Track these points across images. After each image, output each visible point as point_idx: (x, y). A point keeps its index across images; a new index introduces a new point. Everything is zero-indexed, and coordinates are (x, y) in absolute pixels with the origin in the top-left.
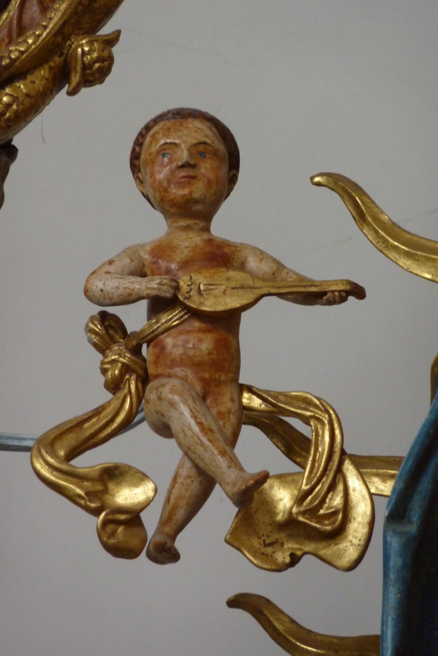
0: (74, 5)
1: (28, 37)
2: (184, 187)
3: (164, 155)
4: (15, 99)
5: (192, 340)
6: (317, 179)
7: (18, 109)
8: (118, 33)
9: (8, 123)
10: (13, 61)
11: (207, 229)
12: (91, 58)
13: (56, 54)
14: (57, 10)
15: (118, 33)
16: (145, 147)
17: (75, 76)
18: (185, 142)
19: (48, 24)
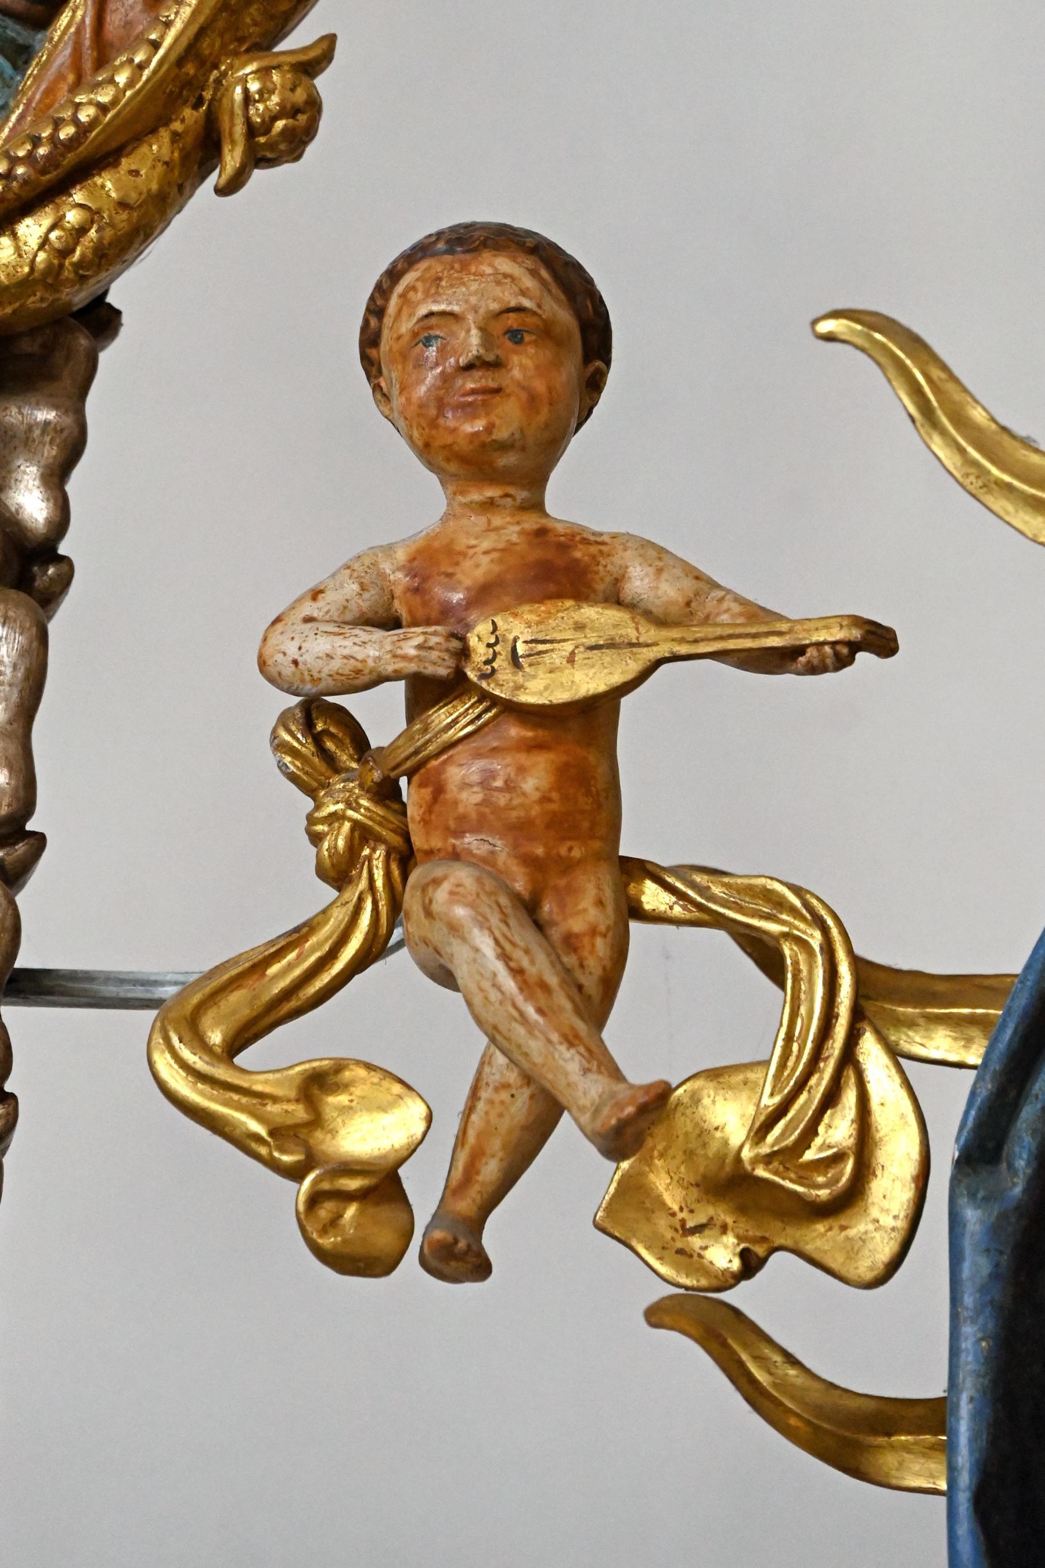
1: (117, 70)
2: (474, 417)
3: (427, 342)
4: (93, 214)
5: (502, 767)
6: (826, 326)
7: (100, 239)
8: (330, 40)
9: (81, 272)
10: (83, 130)
11: (538, 506)
12: (266, 108)
13: (185, 102)
15: (330, 40)
16: (387, 321)
17: (231, 151)
18: (475, 310)
19: (162, 37)
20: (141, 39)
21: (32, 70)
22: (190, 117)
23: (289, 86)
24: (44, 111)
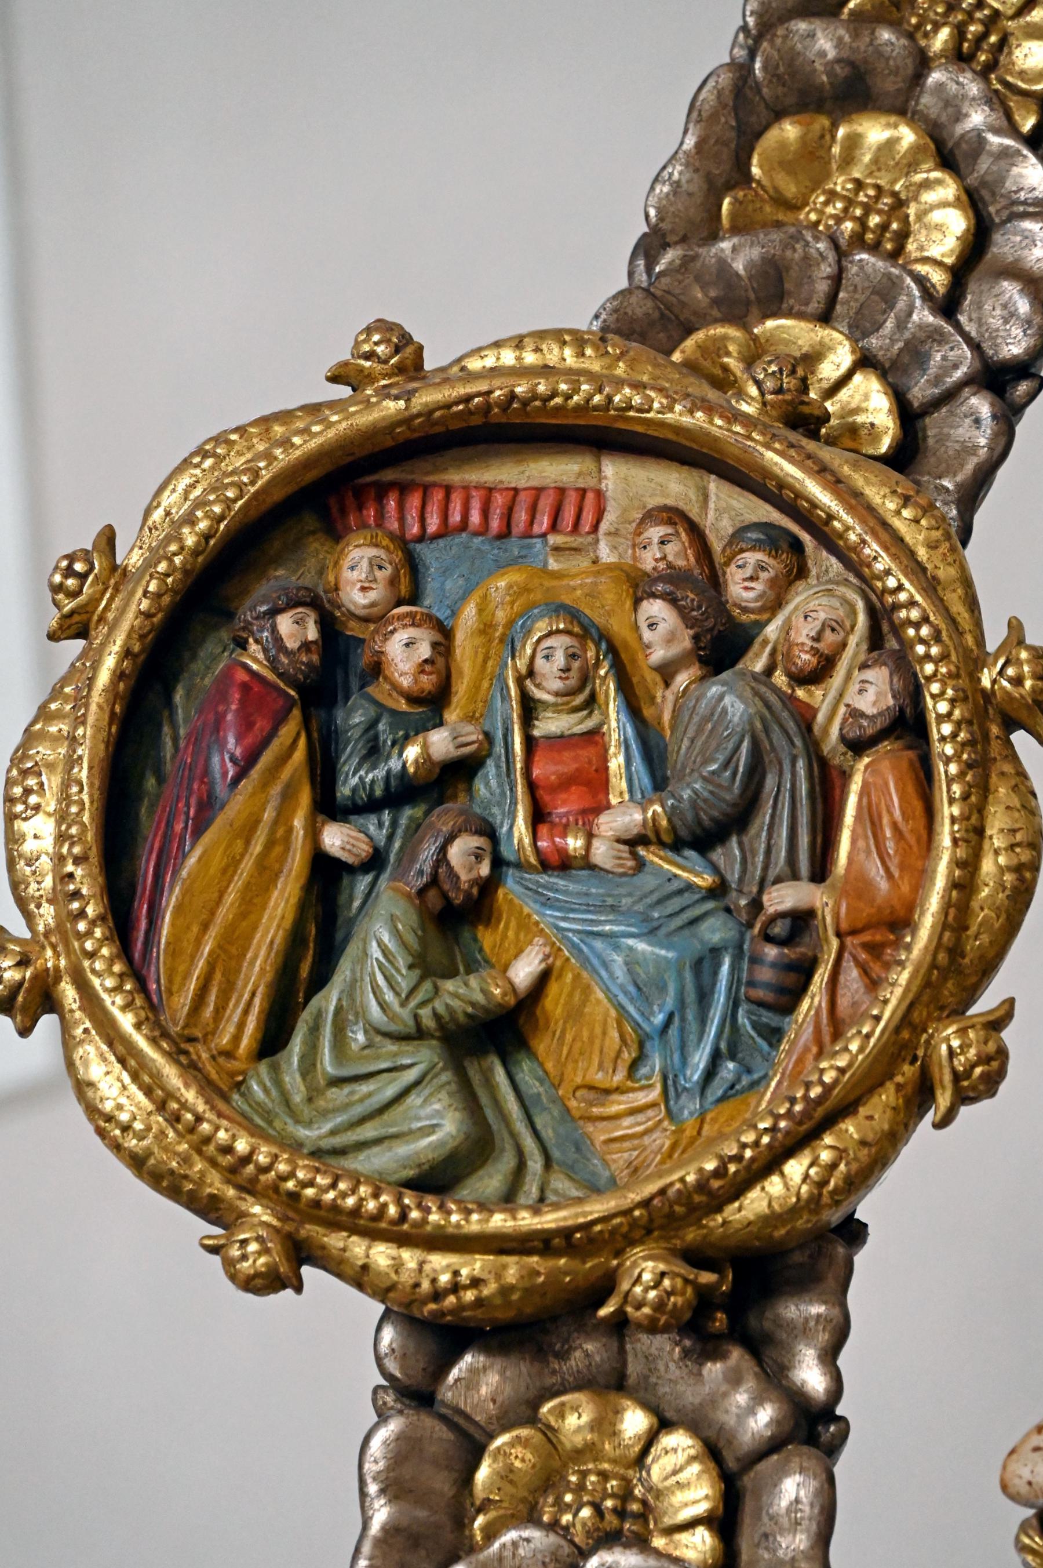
0: (923, 971)
1: (849, 1040)
4: (841, 1153)
7: (849, 1171)
8: (1011, 1002)
10: (828, 1089)
12: (967, 1059)
13: (904, 1060)
14: (893, 984)
15: (1011, 1002)
19: (882, 1012)
20: (865, 1015)
21: (784, 1046)
22: (908, 1071)
23: (982, 1039)
24: (795, 1076)
